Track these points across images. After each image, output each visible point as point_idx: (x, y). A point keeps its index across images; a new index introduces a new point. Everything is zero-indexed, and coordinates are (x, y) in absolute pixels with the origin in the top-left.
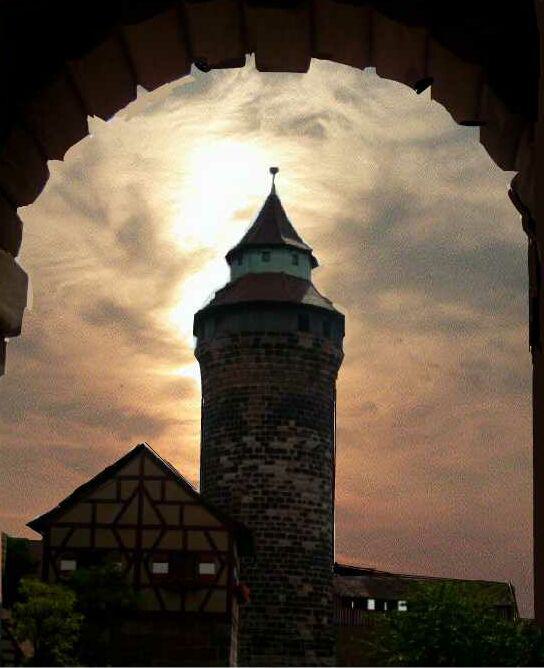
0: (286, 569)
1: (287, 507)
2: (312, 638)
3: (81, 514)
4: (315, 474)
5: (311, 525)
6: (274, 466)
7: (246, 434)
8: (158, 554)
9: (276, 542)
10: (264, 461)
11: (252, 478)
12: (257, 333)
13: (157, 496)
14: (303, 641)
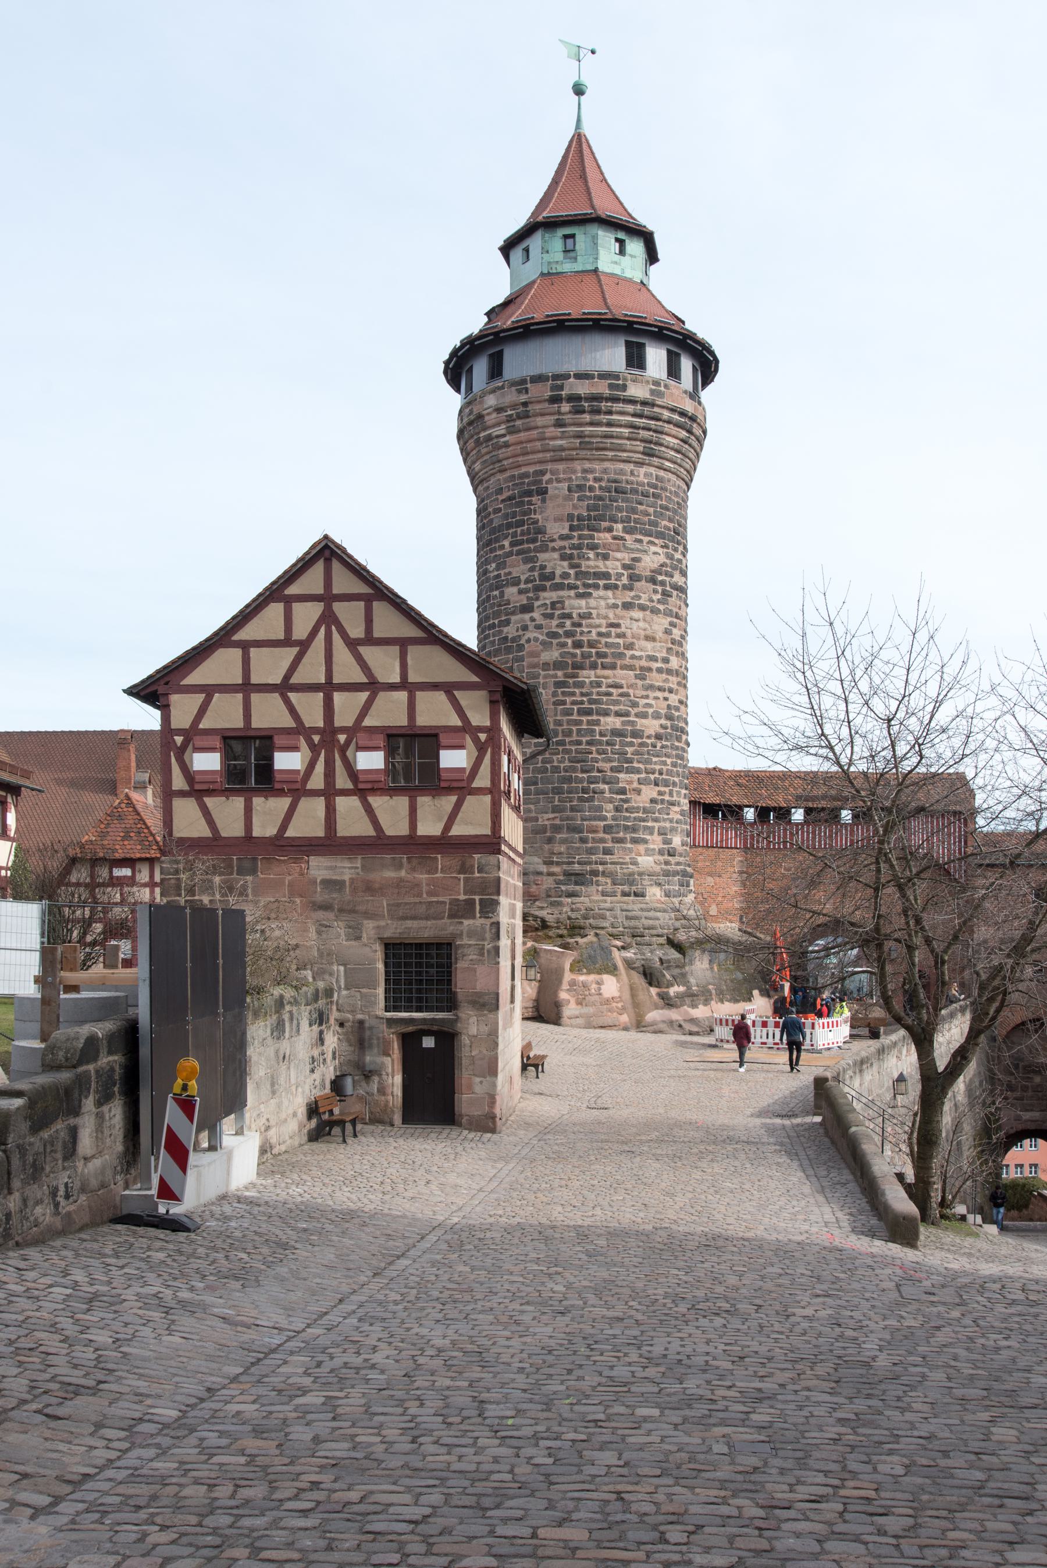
0: (615, 764)
1: (613, 667)
2: (657, 868)
3: (223, 667)
5: (652, 694)
6: (592, 602)
7: (544, 549)
8: (360, 734)
9: (597, 723)
10: (572, 593)
11: (555, 622)
12: (556, 377)
13: (357, 631)
14: (640, 874)
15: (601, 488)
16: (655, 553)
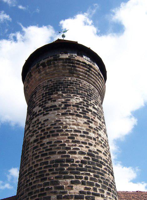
1: (58, 135)
4: (80, 116)
10: (42, 115)
15: (53, 84)
16: (77, 98)
